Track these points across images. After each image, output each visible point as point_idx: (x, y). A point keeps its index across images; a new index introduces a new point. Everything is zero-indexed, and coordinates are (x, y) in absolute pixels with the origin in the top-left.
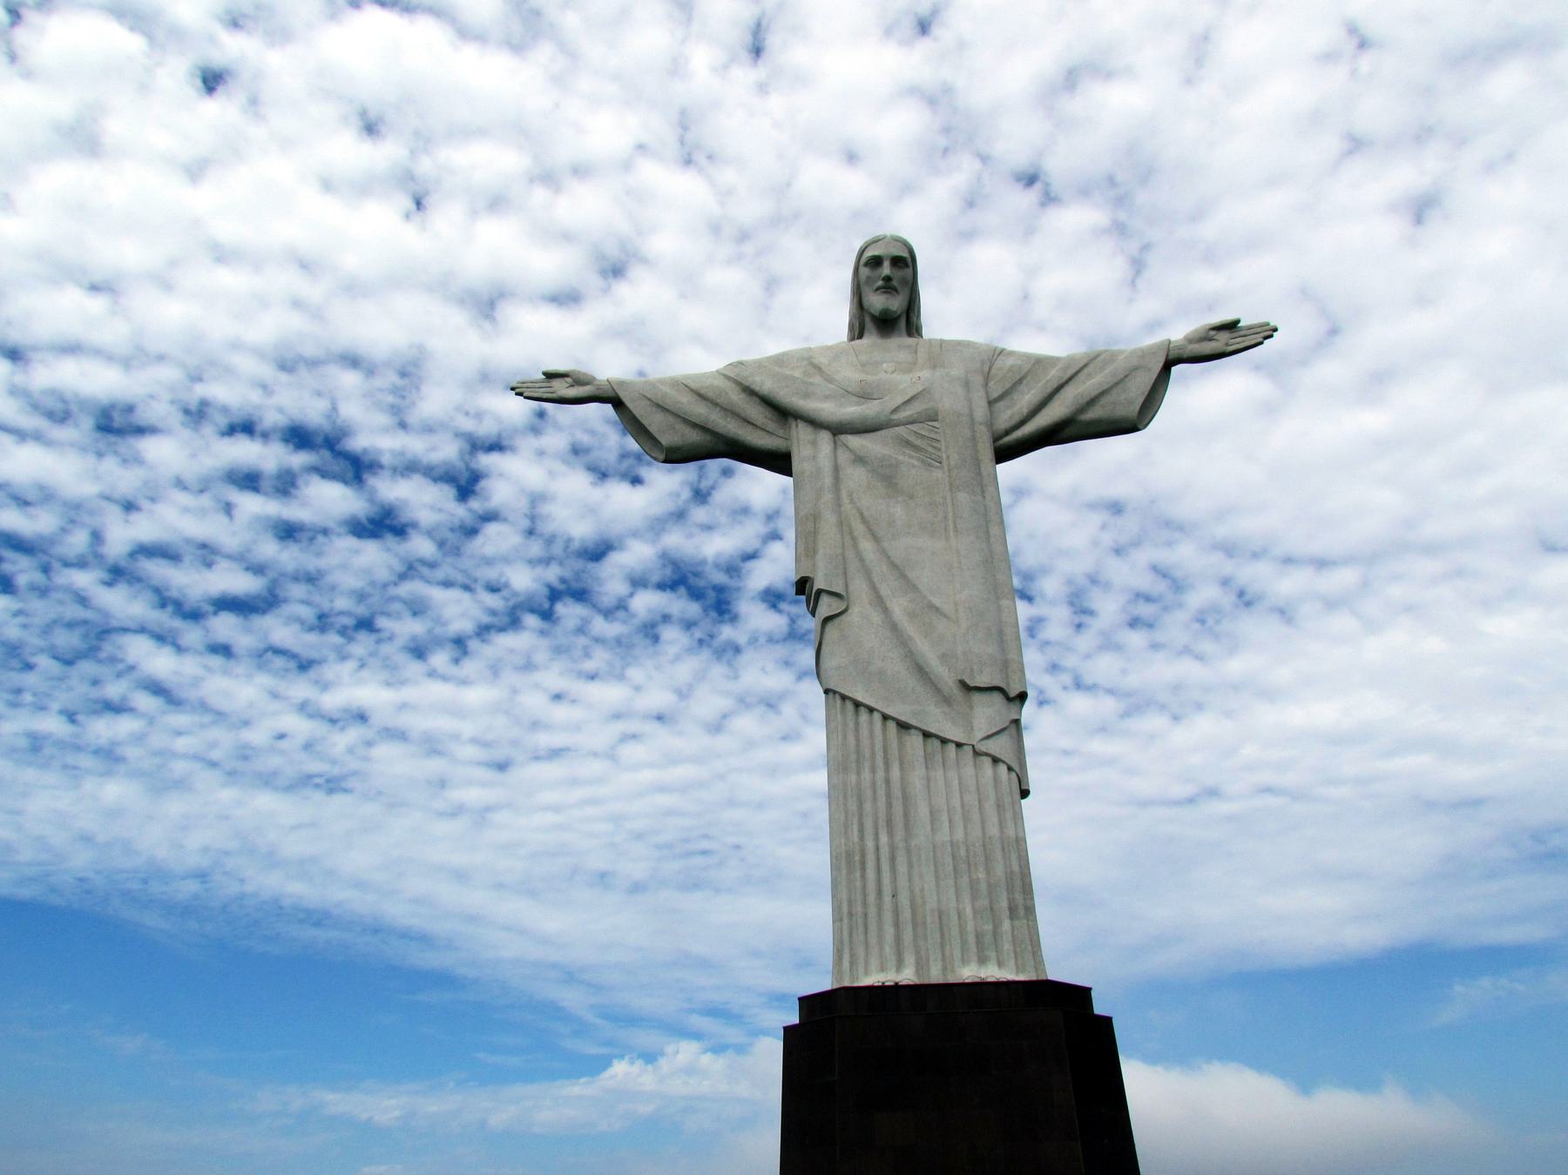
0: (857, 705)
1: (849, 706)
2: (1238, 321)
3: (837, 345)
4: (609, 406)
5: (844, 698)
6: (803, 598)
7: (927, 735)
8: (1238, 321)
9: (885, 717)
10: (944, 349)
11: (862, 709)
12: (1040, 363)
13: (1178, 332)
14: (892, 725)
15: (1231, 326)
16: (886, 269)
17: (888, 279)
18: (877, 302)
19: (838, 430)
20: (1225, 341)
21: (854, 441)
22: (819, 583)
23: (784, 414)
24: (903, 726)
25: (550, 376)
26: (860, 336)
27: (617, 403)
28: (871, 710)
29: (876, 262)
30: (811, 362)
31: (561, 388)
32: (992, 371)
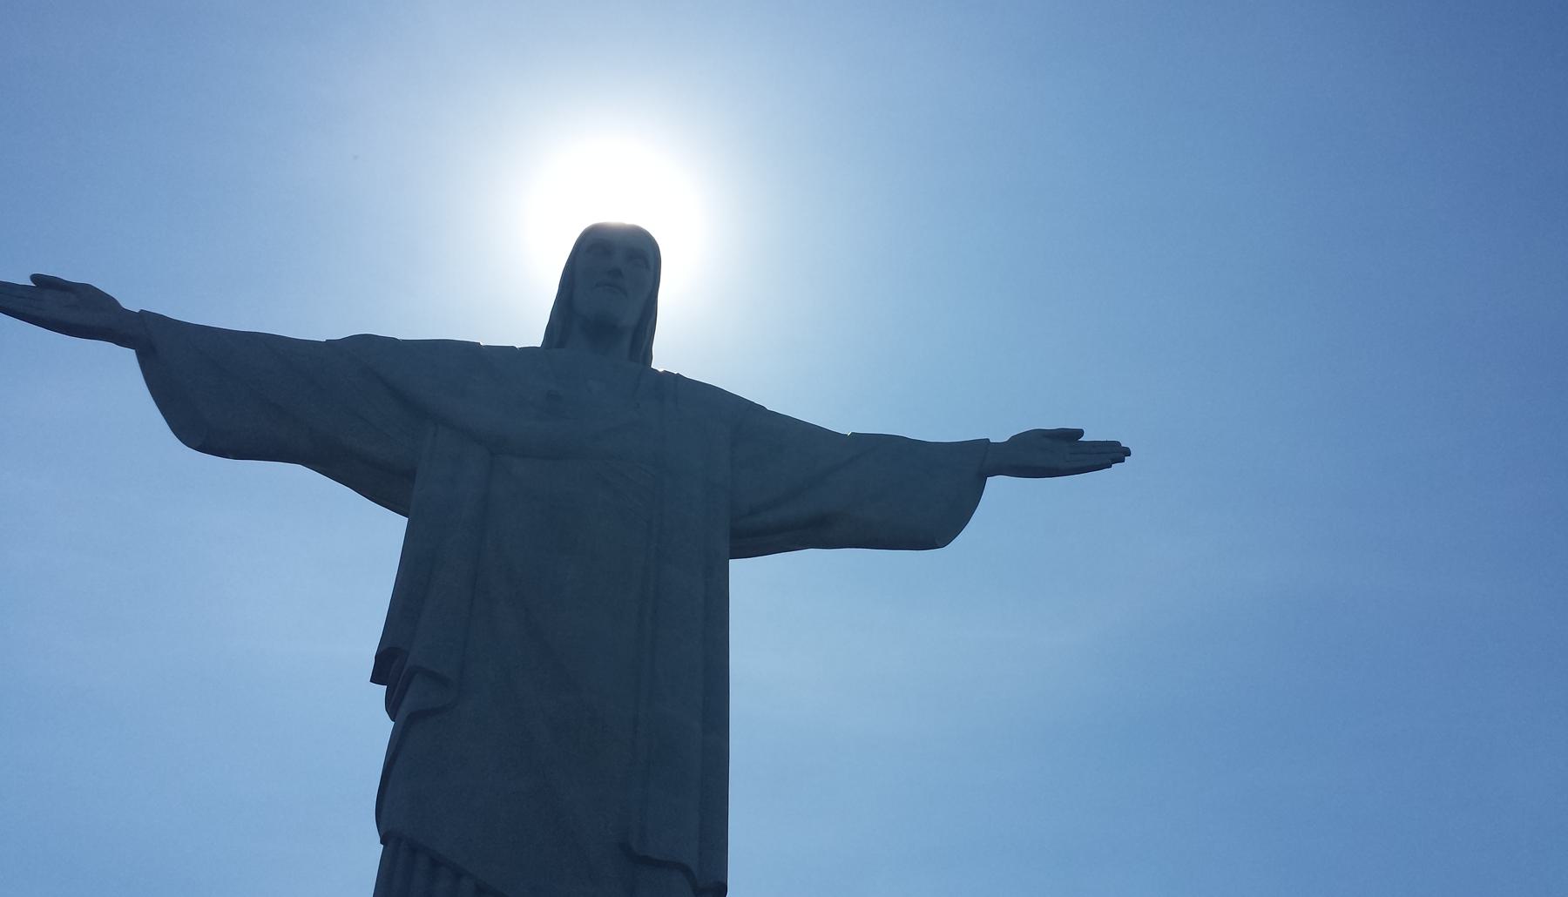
2: (1080, 433)
4: (129, 355)
6: (382, 690)
8: (1080, 433)
13: (1000, 436)
17: (617, 273)
25: (43, 282)
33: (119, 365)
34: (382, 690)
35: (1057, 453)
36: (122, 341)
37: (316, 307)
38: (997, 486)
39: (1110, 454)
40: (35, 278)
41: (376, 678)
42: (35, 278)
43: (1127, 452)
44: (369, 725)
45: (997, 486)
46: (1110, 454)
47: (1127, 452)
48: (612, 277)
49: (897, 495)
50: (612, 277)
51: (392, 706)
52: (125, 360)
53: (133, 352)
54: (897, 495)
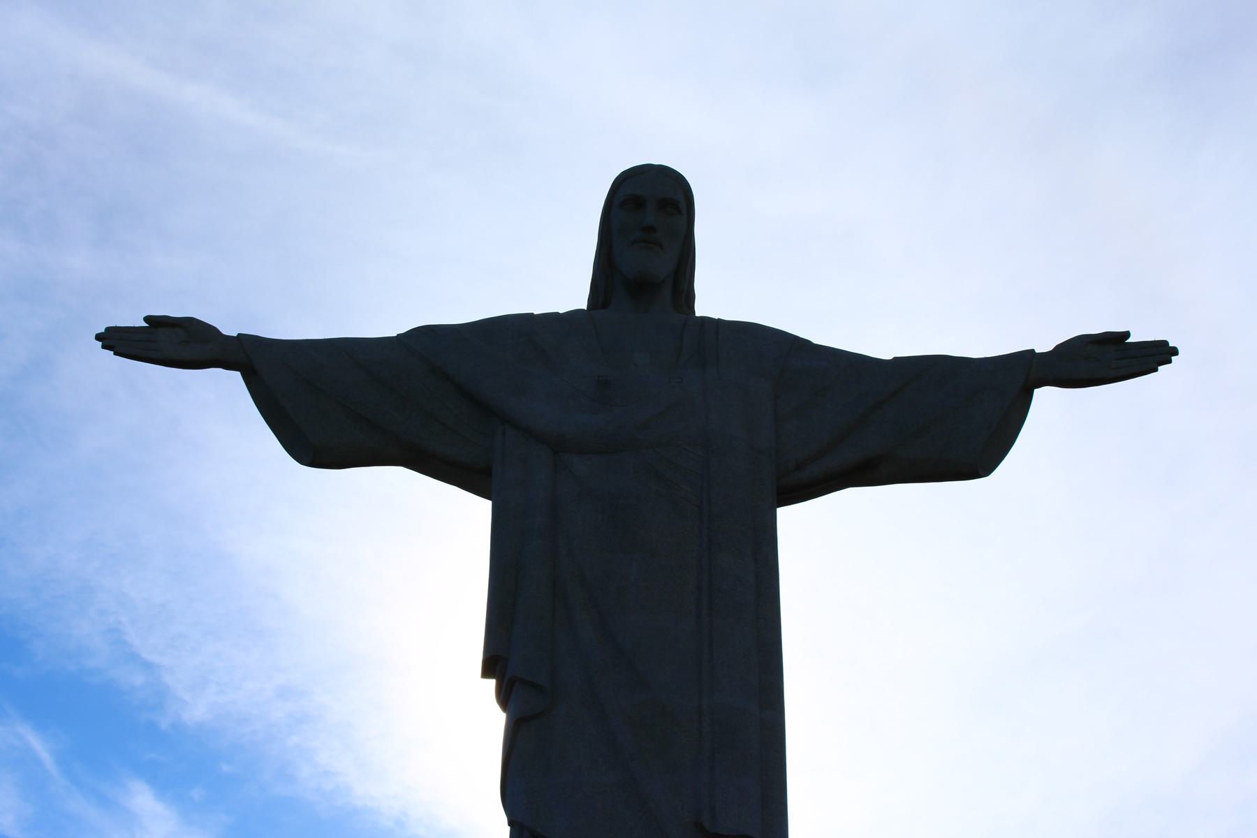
2: (1127, 334)
4: (236, 376)
6: (492, 683)
8: (1127, 334)
13: (1044, 344)
17: (651, 229)
20: (1106, 359)
25: (154, 322)
26: (605, 306)
33: (227, 387)
34: (492, 683)
35: (1106, 359)
37: (380, 311)
40: (147, 319)
41: (487, 672)
42: (147, 319)
43: (1175, 352)
45: (1046, 399)
47: (1175, 352)
48: (648, 218)
49: (944, 419)
50: (648, 218)
51: (504, 698)
52: (235, 378)
53: (238, 373)
54: (944, 419)
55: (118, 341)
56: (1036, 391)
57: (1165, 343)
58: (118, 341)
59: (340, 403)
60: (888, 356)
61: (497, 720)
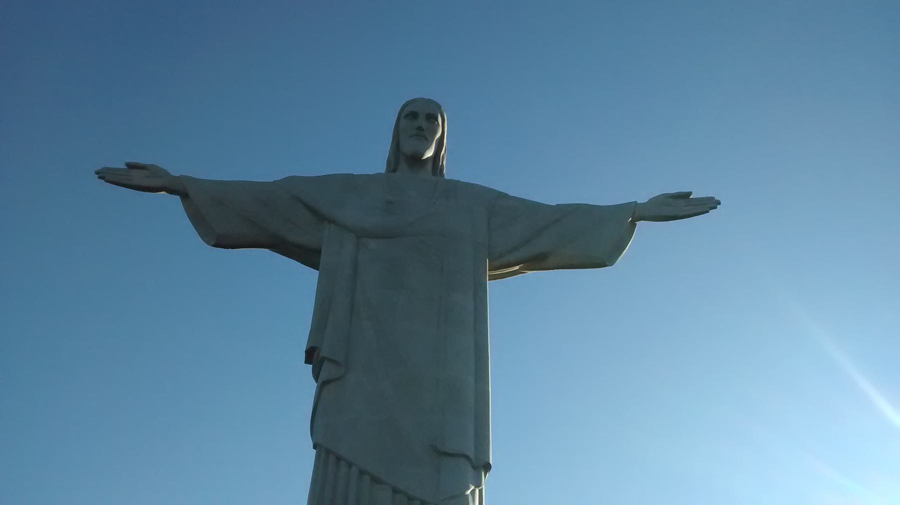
0: (339, 459)
1: (332, 458)
2: (690, 193)
3: (376, 178)
4: (177, 198)
5: (328, 452)
7: (395, 491)
8: (690, 193)
9: (362, 472)
10: (456, 186)
11: (343, 463)
12: (534, 208)
13: (642, 198)
14: (367, 478)
15: (686, 196)
16: (422, 122)
17: (420, 128)
18: (408, 147)
19: (361, 235)
20: (679, 207)
21: (373, 244)
22: (325, 352)
23: (321, 218)
24: (375, 480)
25: (131, 166)
26: (395, 171)
27: (185, 196)
28: (350, 465)
29: (414, 115)
30: (348, 184)
31: (138, 177)
32: (497, 207)
36: (171, 191)
38: (642, 226)
39: (709, 205)
41: (308, 360)
44: (304, 386)
46: (709, 205)
47: (719, 203)
51: (316, 376)
55: (106, 175)
56: (640, 224)
57: (711, 199)
58: (106, 175)
59: (237, 219)
60: (553, 203)
61: (312, 386)
